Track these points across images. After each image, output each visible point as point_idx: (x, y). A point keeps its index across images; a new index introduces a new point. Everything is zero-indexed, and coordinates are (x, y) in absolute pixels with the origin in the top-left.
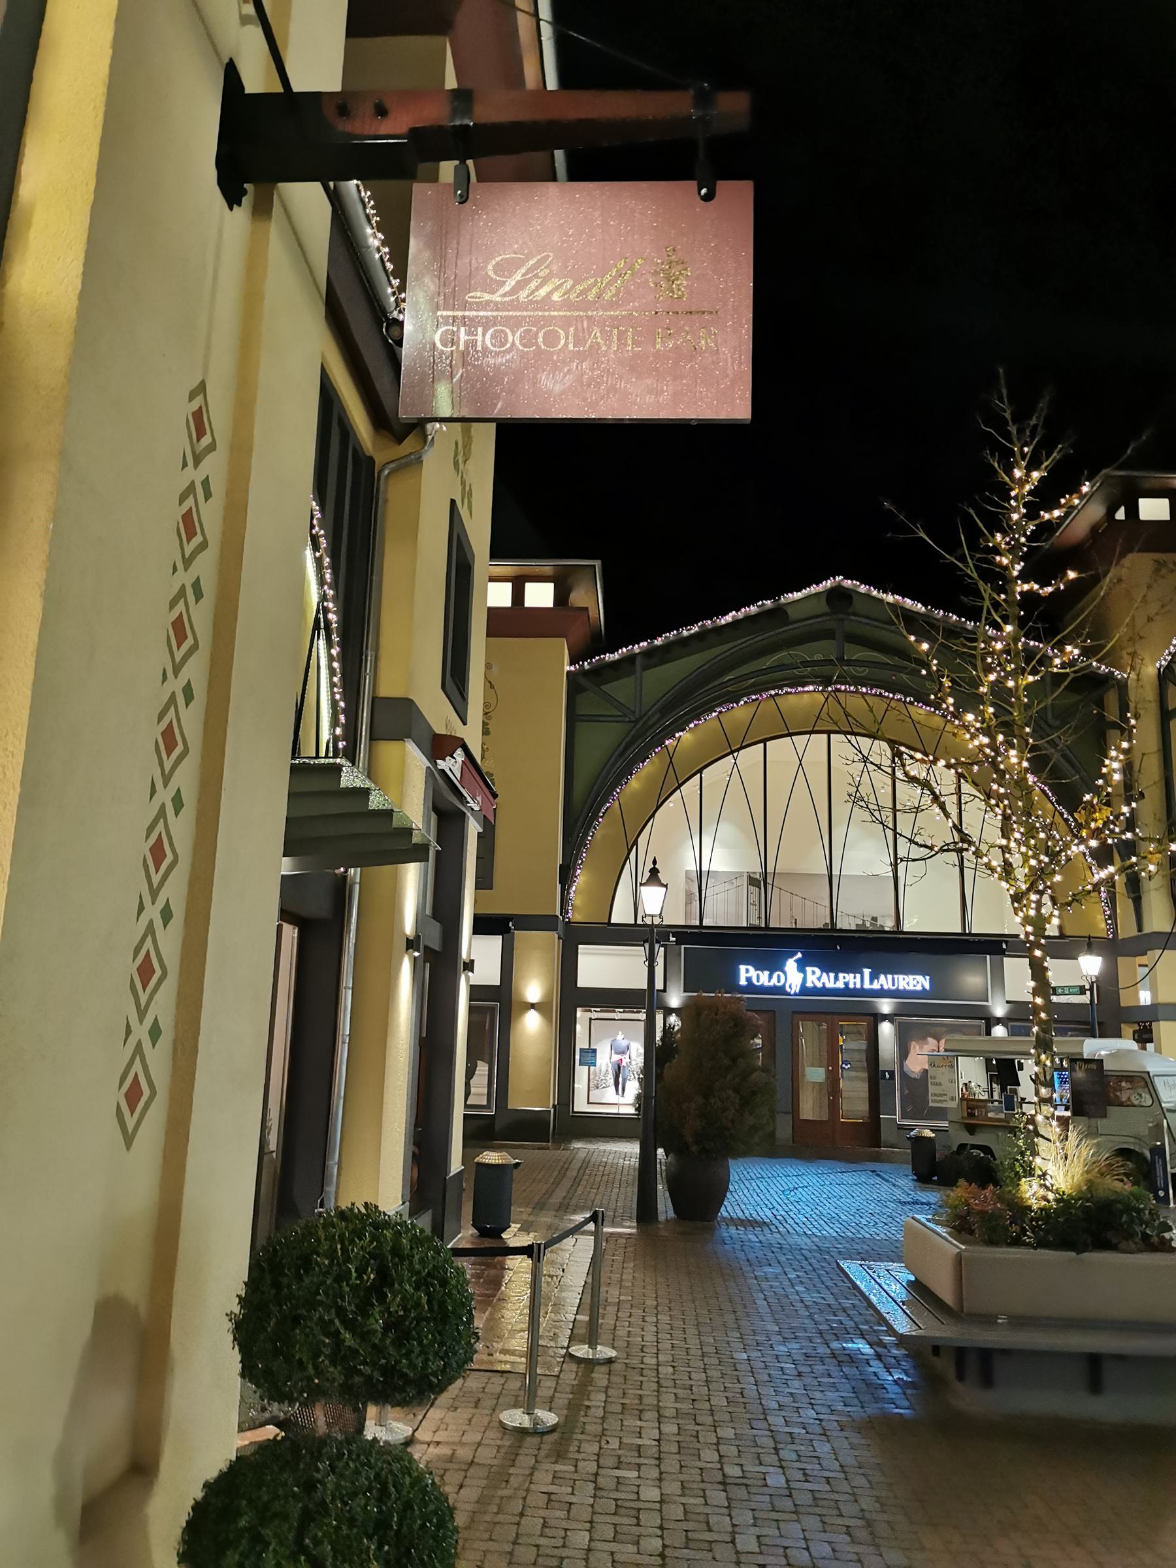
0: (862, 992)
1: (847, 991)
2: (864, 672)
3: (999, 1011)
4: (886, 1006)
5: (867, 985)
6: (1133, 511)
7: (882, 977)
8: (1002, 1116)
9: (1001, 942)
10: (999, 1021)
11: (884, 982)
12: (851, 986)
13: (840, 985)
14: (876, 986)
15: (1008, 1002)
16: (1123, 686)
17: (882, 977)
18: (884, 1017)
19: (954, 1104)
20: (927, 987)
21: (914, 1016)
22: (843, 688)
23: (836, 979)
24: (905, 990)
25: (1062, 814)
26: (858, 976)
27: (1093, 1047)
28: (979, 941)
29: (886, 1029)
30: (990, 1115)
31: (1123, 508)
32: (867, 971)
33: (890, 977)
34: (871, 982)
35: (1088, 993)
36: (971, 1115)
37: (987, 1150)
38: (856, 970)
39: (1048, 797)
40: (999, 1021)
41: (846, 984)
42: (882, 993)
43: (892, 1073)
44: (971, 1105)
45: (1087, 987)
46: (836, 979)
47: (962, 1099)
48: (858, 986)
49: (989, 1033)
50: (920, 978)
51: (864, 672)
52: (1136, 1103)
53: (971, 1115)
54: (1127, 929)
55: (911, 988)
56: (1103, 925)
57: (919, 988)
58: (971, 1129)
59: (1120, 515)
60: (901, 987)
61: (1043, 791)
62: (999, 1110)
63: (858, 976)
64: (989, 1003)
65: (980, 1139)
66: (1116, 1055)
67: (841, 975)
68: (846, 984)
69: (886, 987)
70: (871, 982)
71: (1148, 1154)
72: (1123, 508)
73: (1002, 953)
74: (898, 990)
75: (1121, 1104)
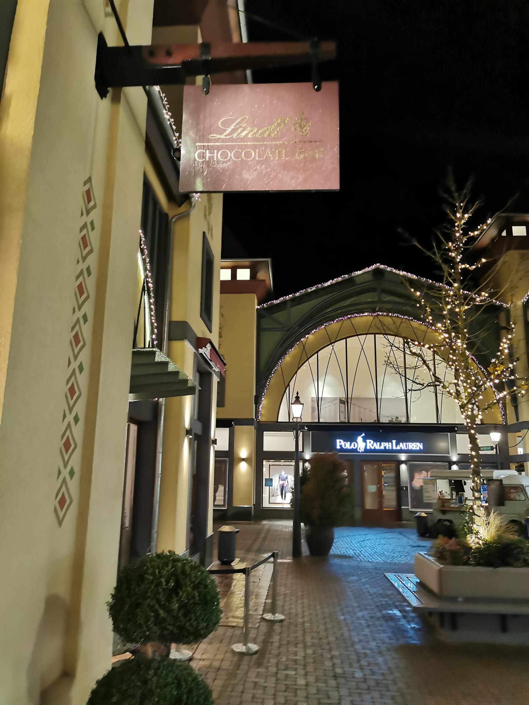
0: (392, 451)
1: (385, 450)
2: (390, 306)
3: (455, 458)
4: (403, 457)
5: (394, 448)
6: (510, 232)
7: (401, 444)
8: (457, 506)
9: (455, 427)
10: (454, 463)
11: (402, 446)
12: (387, 448)
13: (382, 448)
14: (398, 448)
15: (458, 454)
16: (508, 311)
17: (401, 444)
18: (403, 462)
19: (435, 501)
20: (422, 448)
21: (416, 462)
22: (381, 314)
23: (380, 445)
24: (411, 449)
25: (481, 369)
26: (390, 443)
27: (498, 474)
28: (445, 427)
29: (403, 468)
30: (452, 506)
31: (505, 231)
32: (394, 441)
33: (405, 444)
34: (396, 446)
35: (495, 449)
36: (443, 506)
37: (450, 521)
38: (389, 441)
39: (474, 361)
40: (454, 463)
41: (385, 447)
42: (401, 451)
43: (407, 488)
44: (443, 501)
45: (494, 447)
46: (380, 445)
47: (439, 499)
48: (390, 448)
49: (450, 469)
50: (418, 444)
51: (390, 306)
52: (518, 499)
53: (443, 506)
54: (511, 420)
55: (414, 448)
56: (501, 419)
57: (418, 448)
58: (444, 512)
59: (504, 234)
60: (410, 448)
61: (472, 358)
62: (455, 503)
63: (390, 443)
64: (450, 455)
65: (448, 517)
66: (509, 477)
67: (382, 443)
68: (385, 447)
69: (403, 448)
70: (396, 446)
71: (523, 522)
72: (505, 231)
73: (456, 431)
74: (408, 449)
75: (511, 500)
